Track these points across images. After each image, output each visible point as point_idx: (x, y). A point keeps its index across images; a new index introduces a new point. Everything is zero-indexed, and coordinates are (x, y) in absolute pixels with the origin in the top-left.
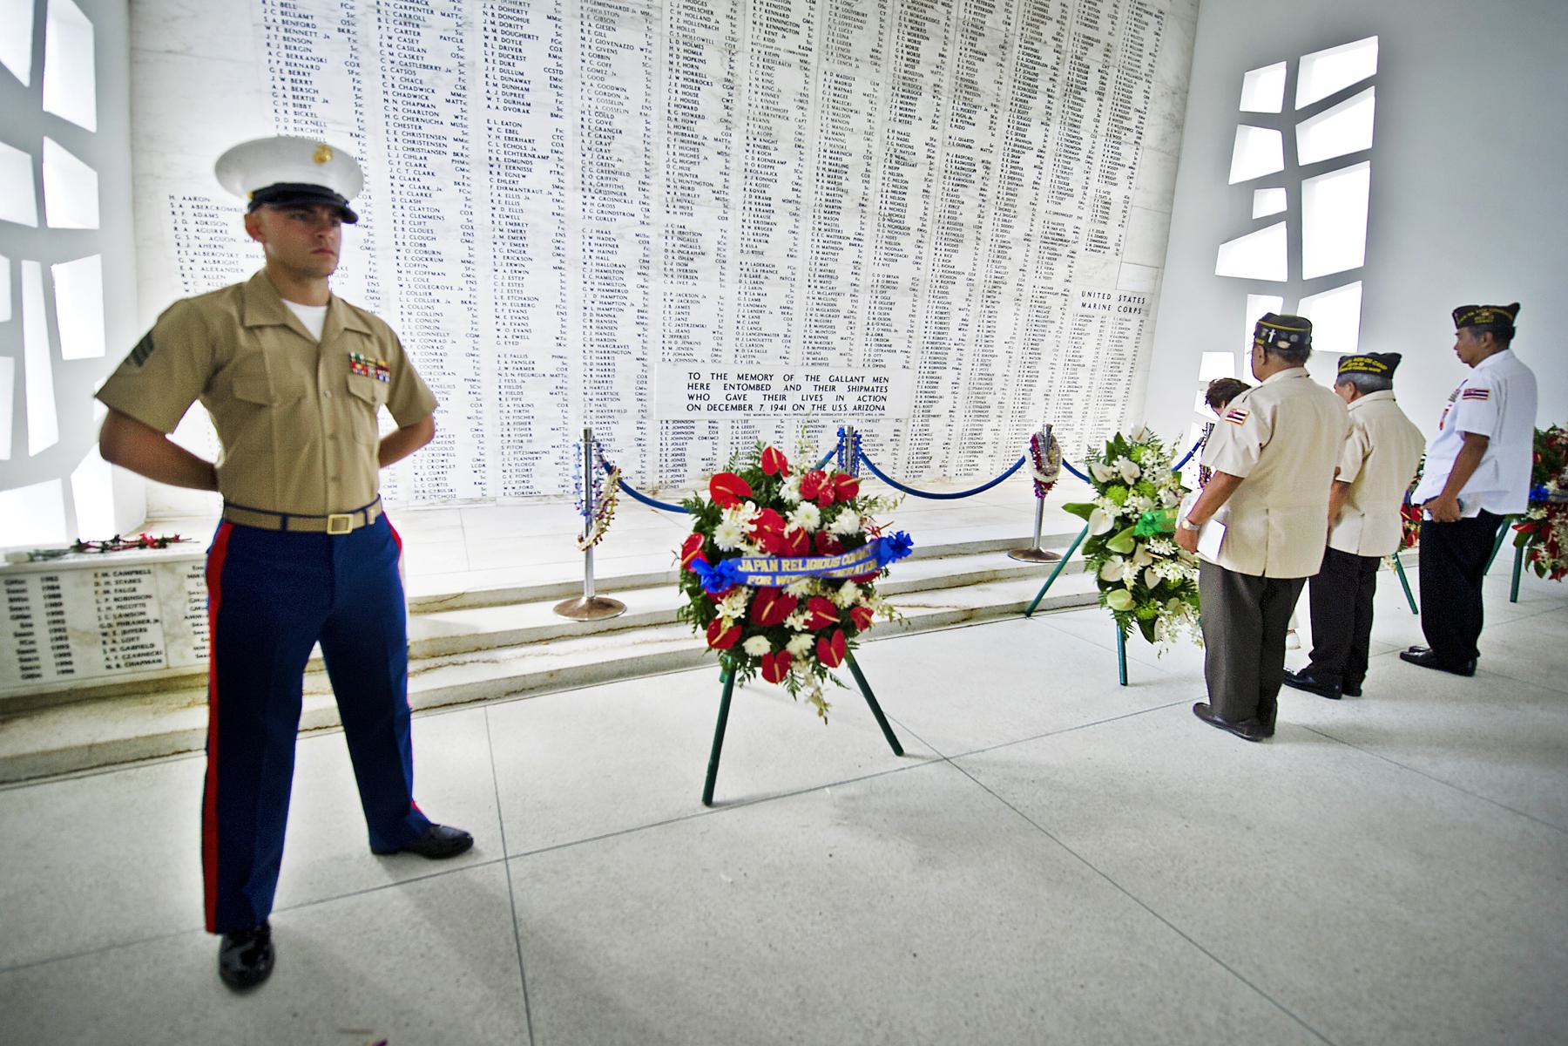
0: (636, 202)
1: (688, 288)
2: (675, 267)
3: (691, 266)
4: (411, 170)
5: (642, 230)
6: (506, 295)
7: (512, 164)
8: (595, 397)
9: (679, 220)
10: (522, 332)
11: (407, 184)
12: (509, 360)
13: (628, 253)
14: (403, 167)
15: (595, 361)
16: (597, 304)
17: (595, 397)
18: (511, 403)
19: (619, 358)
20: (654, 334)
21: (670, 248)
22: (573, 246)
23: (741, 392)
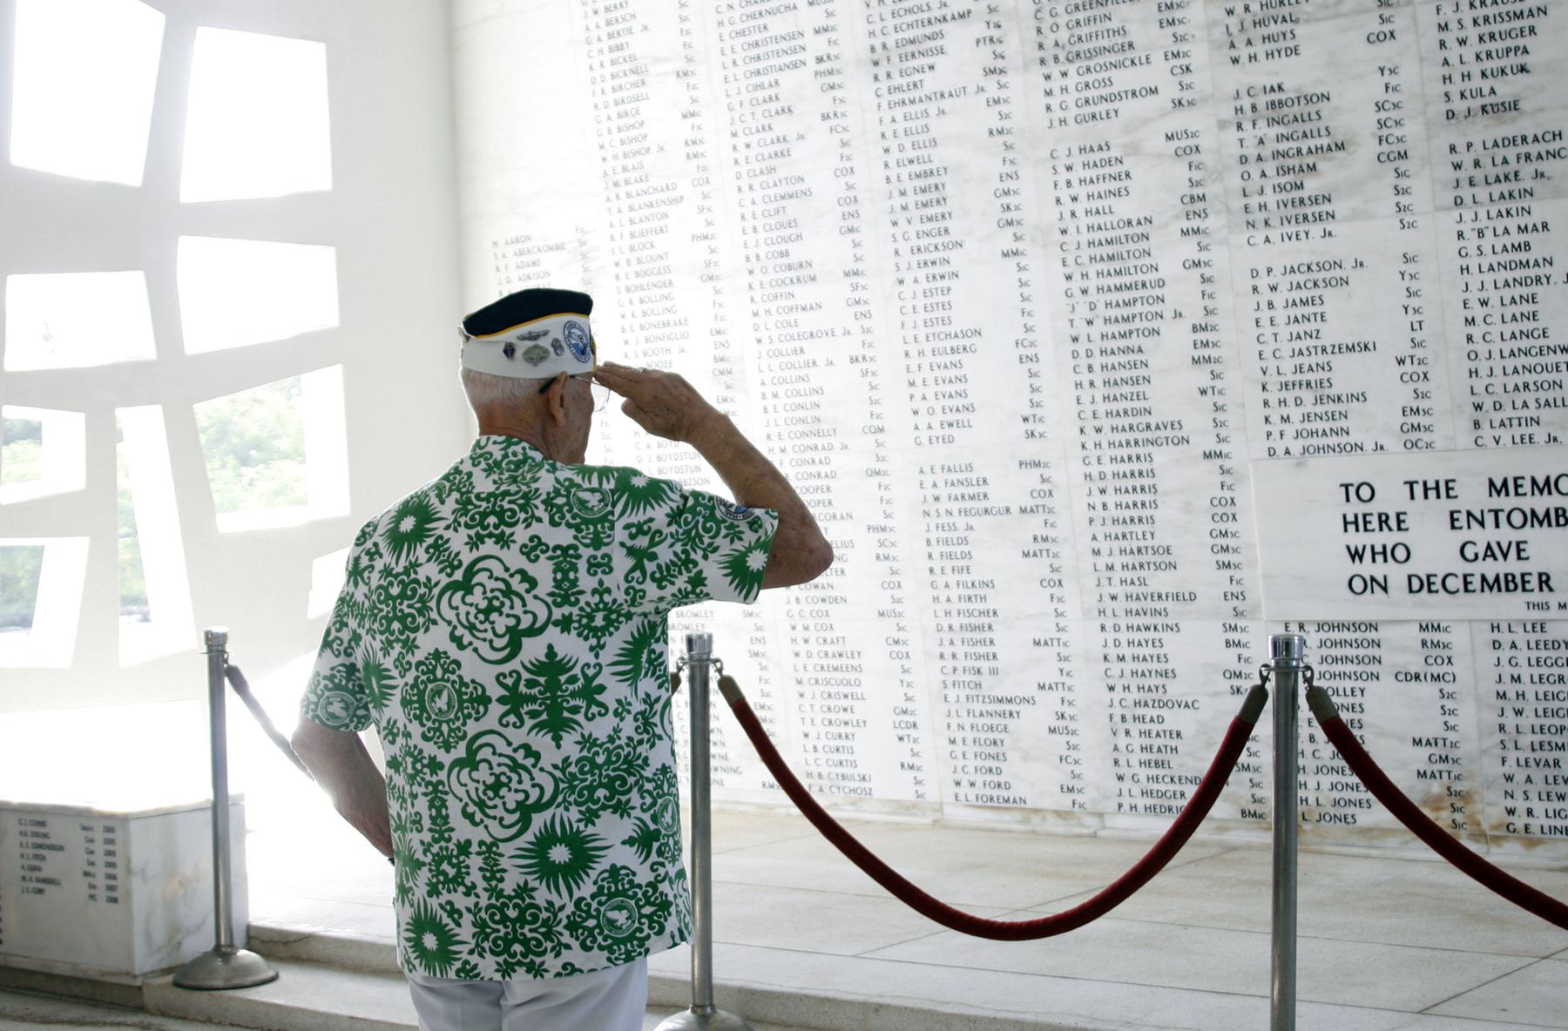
0: (1157, 58)
1: (1312, 247)
2: (1271, 199)
3: (1312, 186)
4: (759, 110)
5: (1178, 121)
6: (922, 332)
7: (911, 49)
8: (1118, 560)
9: (1263, 74)
10: (959, 412)
11: (754, 139)
12: (940, 478)
13: (1154, 187)
14: (748, 109)
15: (1109, 468)
16: (1100, 326)
17: (1118, 560)
18: (952, 579)
19: (1161, 456)
20: (1240, 384)
21: (1251, 151)
22: (1037, 200)
23: (1506, 535)
